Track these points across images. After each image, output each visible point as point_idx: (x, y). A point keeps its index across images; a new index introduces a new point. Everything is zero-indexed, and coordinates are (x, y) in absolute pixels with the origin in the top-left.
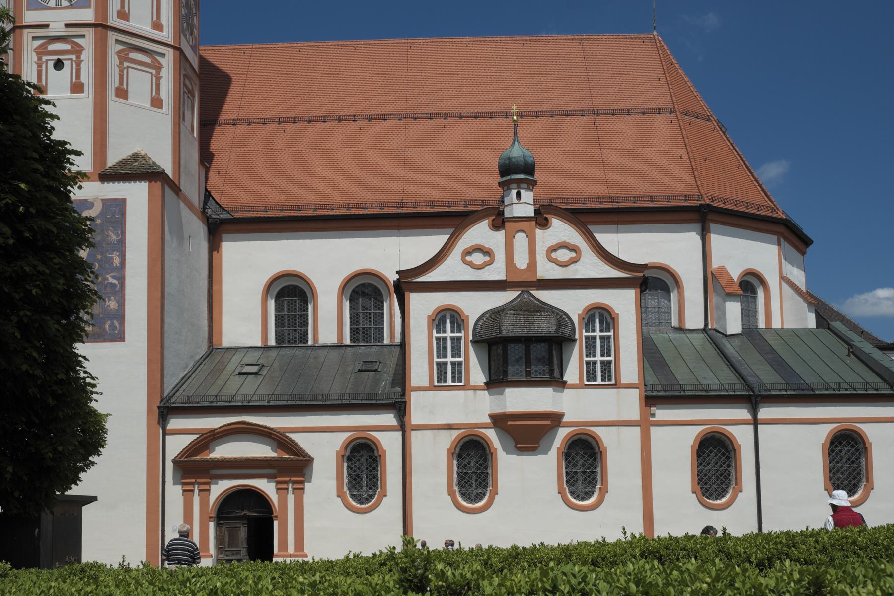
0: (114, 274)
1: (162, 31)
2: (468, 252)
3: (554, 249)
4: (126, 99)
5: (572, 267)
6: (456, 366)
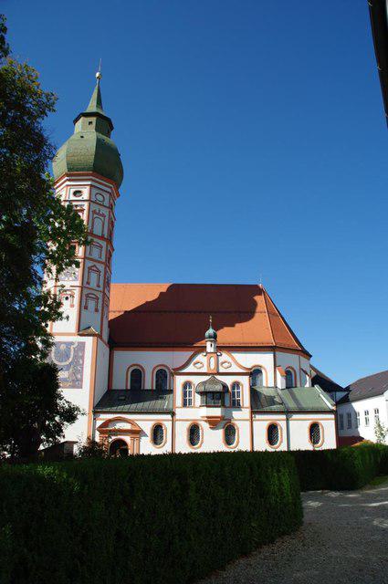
2: (195, 364)
6: (190, 400)
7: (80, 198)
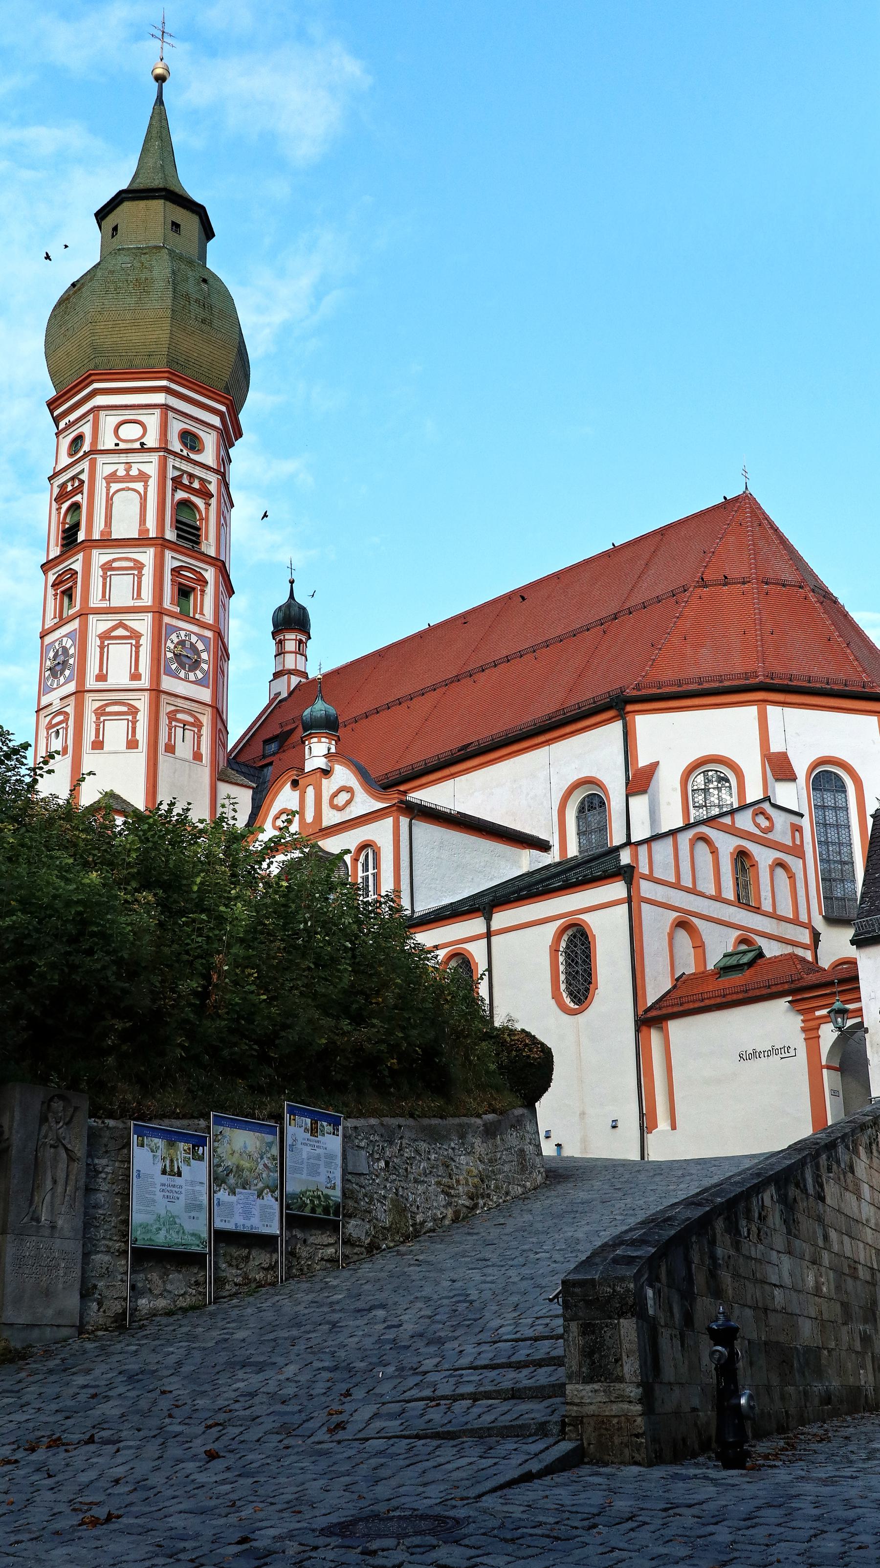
1: (140, 679)
2: (277, 817)
3: (335, 795)
4: (102, 748)
5: (348, 809)
7: (81, 454)
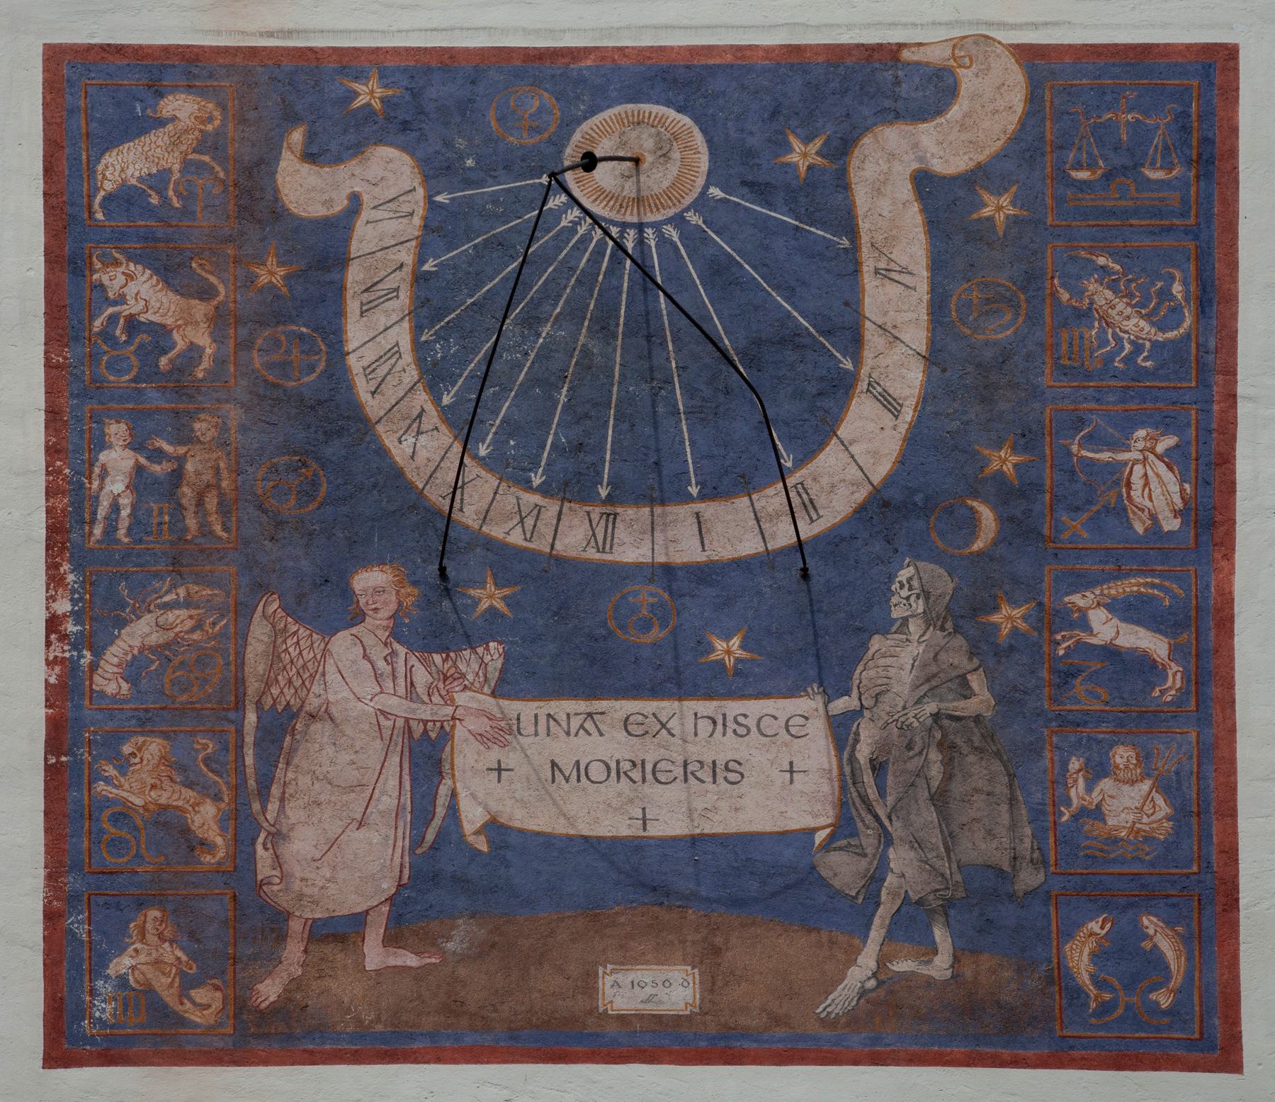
0: (1130, 586)
